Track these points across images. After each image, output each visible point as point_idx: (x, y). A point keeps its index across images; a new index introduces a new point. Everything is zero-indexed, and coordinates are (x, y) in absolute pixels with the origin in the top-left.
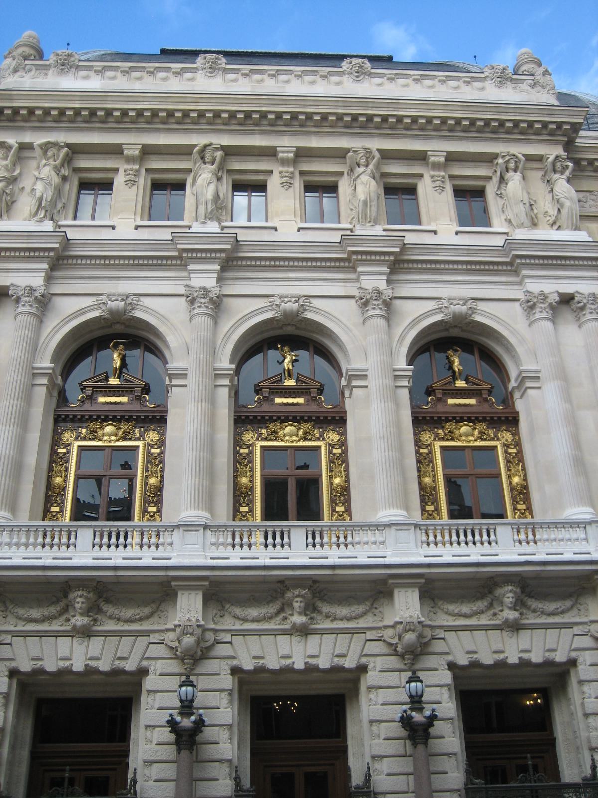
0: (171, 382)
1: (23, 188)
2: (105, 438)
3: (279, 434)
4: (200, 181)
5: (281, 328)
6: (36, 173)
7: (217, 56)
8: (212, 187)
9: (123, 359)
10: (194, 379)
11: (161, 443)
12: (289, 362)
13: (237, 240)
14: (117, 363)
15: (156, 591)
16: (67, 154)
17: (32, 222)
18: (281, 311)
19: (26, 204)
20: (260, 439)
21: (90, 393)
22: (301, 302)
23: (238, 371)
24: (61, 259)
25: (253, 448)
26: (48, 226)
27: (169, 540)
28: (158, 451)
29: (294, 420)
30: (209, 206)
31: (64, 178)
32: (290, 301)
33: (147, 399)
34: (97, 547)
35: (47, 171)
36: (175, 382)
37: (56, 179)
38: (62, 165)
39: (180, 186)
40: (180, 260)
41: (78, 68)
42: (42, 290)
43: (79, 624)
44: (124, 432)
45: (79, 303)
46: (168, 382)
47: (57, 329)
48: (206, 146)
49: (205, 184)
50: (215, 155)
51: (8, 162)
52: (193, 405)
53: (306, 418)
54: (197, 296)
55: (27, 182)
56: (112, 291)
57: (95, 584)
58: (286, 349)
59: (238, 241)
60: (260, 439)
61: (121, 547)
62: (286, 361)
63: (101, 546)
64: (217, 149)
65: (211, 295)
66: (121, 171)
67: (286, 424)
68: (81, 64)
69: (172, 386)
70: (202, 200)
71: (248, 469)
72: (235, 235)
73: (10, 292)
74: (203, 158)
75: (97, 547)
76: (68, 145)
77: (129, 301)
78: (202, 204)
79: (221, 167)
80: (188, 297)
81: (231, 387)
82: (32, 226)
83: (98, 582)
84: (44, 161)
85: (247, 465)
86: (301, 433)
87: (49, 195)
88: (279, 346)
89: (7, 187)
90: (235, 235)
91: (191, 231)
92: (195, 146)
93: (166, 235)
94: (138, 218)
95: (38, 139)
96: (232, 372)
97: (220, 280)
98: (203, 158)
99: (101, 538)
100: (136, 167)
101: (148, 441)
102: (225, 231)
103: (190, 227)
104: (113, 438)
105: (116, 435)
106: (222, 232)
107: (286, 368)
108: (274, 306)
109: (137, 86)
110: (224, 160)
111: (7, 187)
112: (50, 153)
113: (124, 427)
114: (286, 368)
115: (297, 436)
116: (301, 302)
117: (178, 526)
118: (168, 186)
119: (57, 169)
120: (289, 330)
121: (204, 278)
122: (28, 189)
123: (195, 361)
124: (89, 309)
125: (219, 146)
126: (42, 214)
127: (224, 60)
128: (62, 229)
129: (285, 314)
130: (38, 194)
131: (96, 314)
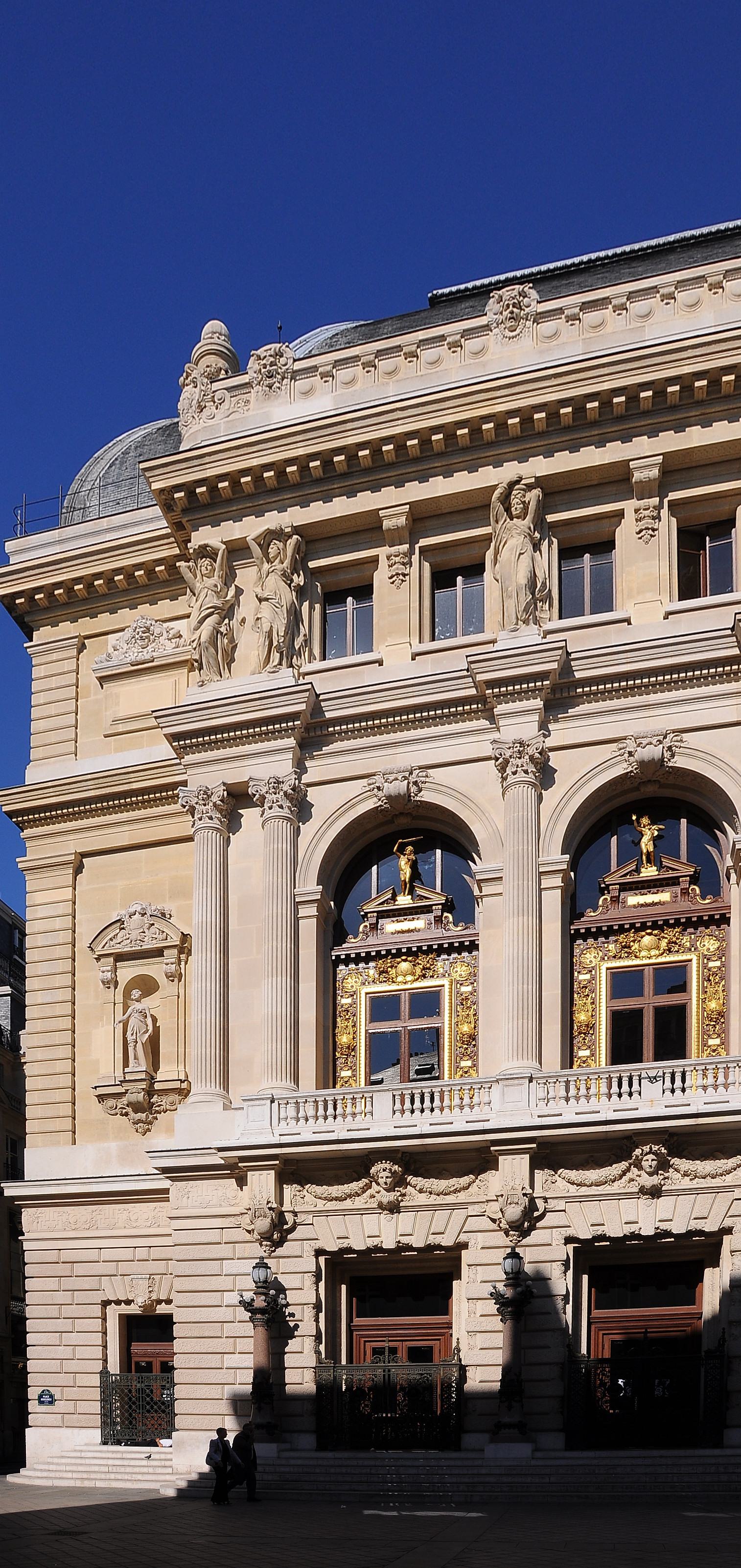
0: (481, 892)
1: (243, 621)
2: (400, 979)
3: (633, 948)
4: (505, 554)
5: (637, 789)
6: (258, 590)
7: (522, 287)
8: (525, 560)
9: (414, 866)
10: (512, 883)
11: (472, 978)
12: (649, 840)
13: (567, 652)
14: (406, 872)
15: (473, 1158)
16: (297, 549)
17: (264, 675)
18: (636, 761)
19: (250, 646)
20: (606, 958)
21: (374, 921)
22: (667, 742)
23: (574, 865)
24: (314, 731)
25: (596, 972)
26: (286, 677)
27: (486, 1099)
28: (469, 988)
29: (655, 926)
30: (522, 597)
31: (301, 593)
32: (651, 744)
33: (451, 919)
34: (398, 1114)
35: (275, 585)
36: (487, 889)
37: (288, 596)
38: (295, 570)
39: (475, 570)
40: (482, 704)
41: (295, 375)
42: (292, 780)
43: (385, 1201)
44: (424, 969)
45: (345, 788)
46: (476, 892)
47: (318, 838)
48: (512, 485)
49: (514, 558)
50: (527, 499)
51: (216, 579)
52: (511, 921)
53: (672, 922)
54: (511, 757)
55: (247, 608)
56: (389, 767)
57: (400, 1155)
58: (645, 821)
59: (568, 654)
60: (606, 958)
61: (427, 1112)
62: (645, 840)
63: (403, 1112)
64: (530, 487)
65: (531, 751)
66: (383, 563)
67: (643, 933)
68: (298, 366)
69: (481, 897)
70: (512, 589)
71: (589, 1000)
72: (563, 644)
73: (250, 791)
74: (508, 510)
75: (398, 1114)
76: (297, 530)
77: (413, 779)
78: (510, 597)
79: (540, 523)
80: (497, 759)
81: (564, 890)
82: (265, 682)
83: (403, 1153)
84: (266, 566)
85: (588, 995)
86: (664, 944)
87: (280, 626)
88: (634, 818)
89: (220, 623)
90: (563, 644)
91: (497, 647)
92: (495, 487)
93: (457, 661)
94: (415, 640)
95: (249, 528)
96: (565, 867)
97: (543, 726)
98: (508, 510)
99: (403, 1103)
100: (405, 547)
101: (456, 976)
102: (550, 638)
103: (493, 642)
104: (409, 978)
105: (413, 974)
106: (544, 641)
107: (645, 851)
108: (626, 755)
109: (392, 390)
110: (544, 507)
111: (220, 623)
112: (272, 551)
113: (423, 960)
114: (645, 851)
115: (658, 948)
116: (667, 742)
117: (497, 1081)
118: (455, 570)
119: (287, 578)
120: (650, 790)
121: (519, 722)
122: (250, 621)
123: (512, 857)
124: (359, 799)
125: (533, 480)
126: (275, 657)
127: (533, 294)
128: (308, 679)
129: (643, 764)
130: (266, 628)
131: (370, 804)
